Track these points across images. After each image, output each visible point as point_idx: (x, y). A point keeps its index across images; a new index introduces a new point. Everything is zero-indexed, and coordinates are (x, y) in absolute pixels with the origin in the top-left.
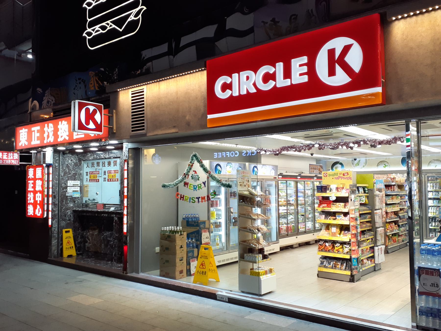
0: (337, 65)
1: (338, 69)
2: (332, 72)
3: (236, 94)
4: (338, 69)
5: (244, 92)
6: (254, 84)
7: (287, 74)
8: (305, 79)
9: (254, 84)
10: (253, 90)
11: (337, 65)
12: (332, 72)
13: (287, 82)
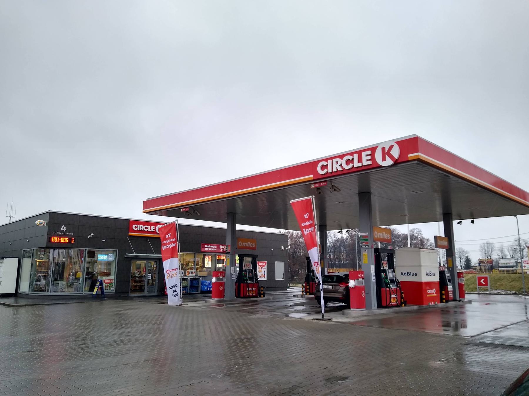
0: (386, 155)
1: (387, 157)
2: (384, 159)
3: (330, 171)
4: (387, 157)
5: (335, 170)
6: (341, 165)
8: (370, 162)
9: (341, 165)
10: (340, 169)
11: (386, 155)
12: (384, 159)
13: (360, 165)
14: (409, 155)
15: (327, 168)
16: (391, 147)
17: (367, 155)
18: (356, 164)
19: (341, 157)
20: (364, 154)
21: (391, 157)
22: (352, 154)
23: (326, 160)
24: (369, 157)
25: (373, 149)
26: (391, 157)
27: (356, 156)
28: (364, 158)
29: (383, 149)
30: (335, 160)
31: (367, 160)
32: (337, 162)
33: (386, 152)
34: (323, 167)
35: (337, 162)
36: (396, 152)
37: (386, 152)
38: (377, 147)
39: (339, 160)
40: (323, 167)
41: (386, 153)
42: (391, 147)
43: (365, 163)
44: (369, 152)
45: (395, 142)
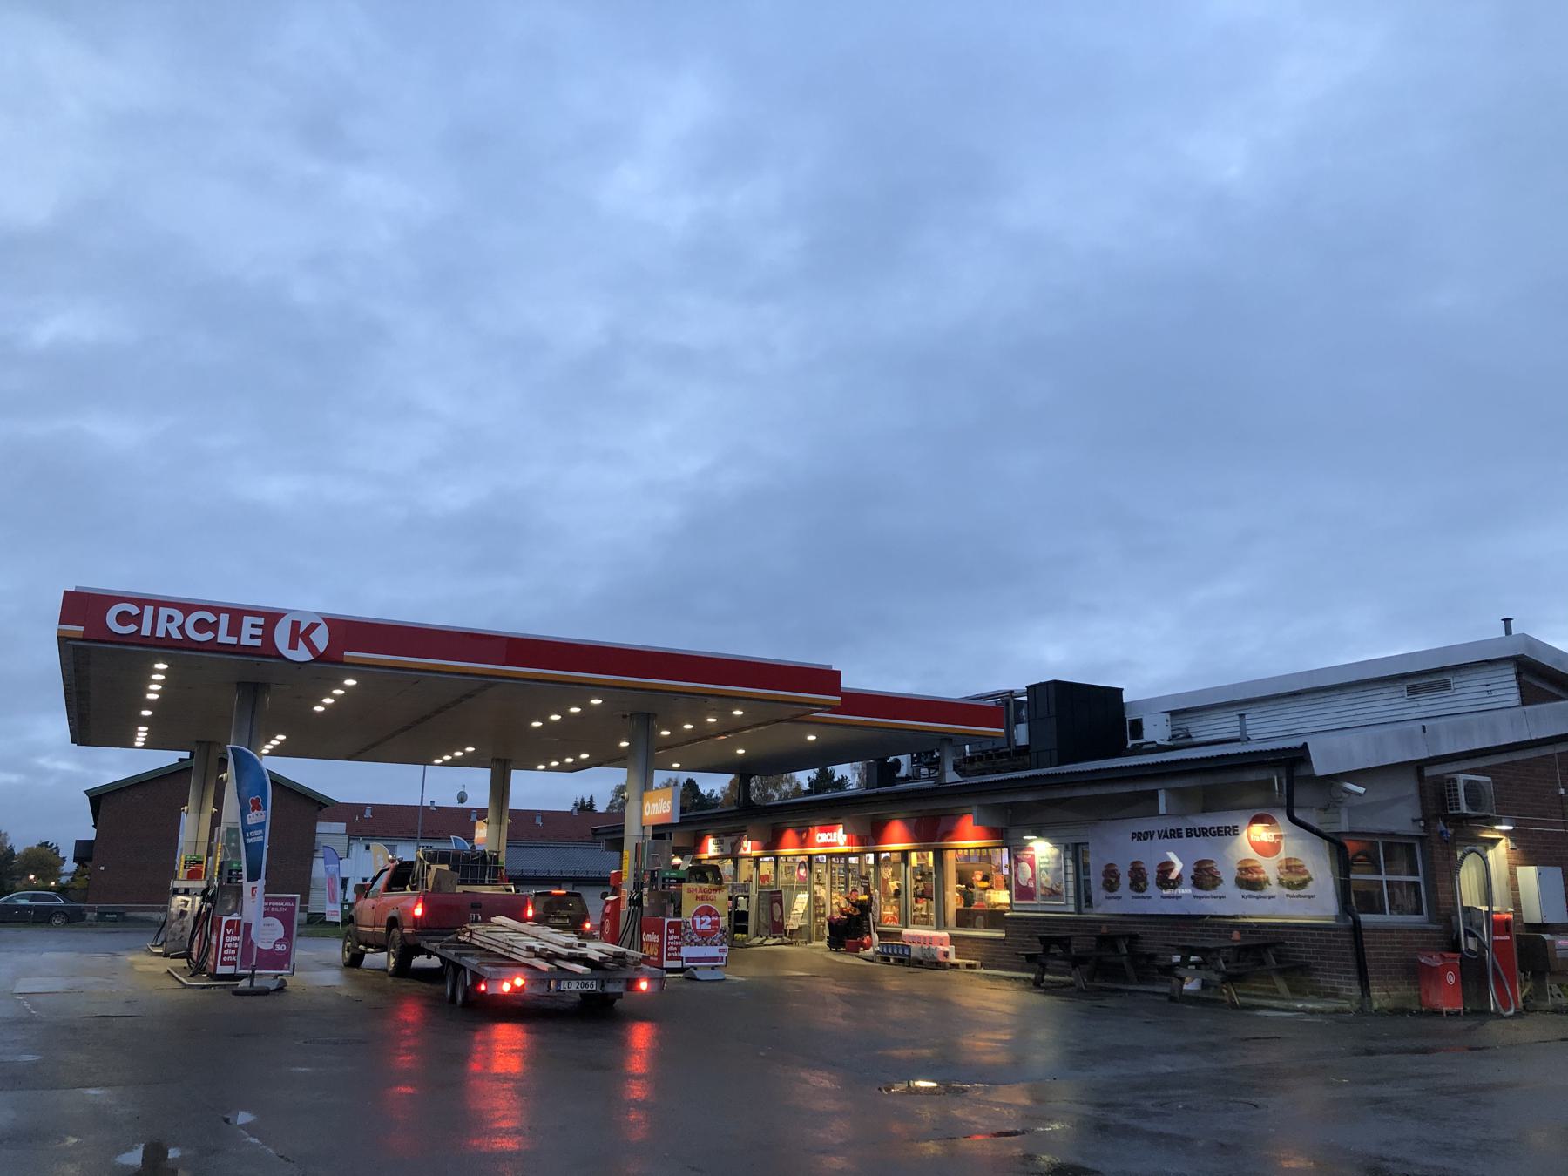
0: (300, 640)
1: (301, 642)
2: (293, 645)
3: (146, 631)
4: (301, 642)
5: (160, 633)
6: (181, 628)
7: (235, 629)
8: (258, 643)
9: (181, 628)
10: (176, 635)
11: (300, 640)
12: (293, 645)
13: (233, 640)
14: (346, 653)
15: (139, 625)
16: (313, 627)
17: (253, 626)
18: (223, 638)
19: (187, 608)
20: (248, 621)
21: (311, 646)
22: (216, 610)
23: (141, 602)
24: (259, 632)
25: (272, 618)
26: (311, 646)
27: (225, 618)
28: (247, 630)
29: (296, 624)
30: (164, 612)
31: (252, 636)
32: (170, 619)
33: (301, 632)
34: (123, 618)
35: (170, 619)
36: (321, 639)
37: (301, 632)
38: (284, 615)
39: (178, 615)
40: (123, 618)
41: (300, 634)
42: (313, 627)
43: (246, 640)
44: (261, 621)
45: (324, 619)
